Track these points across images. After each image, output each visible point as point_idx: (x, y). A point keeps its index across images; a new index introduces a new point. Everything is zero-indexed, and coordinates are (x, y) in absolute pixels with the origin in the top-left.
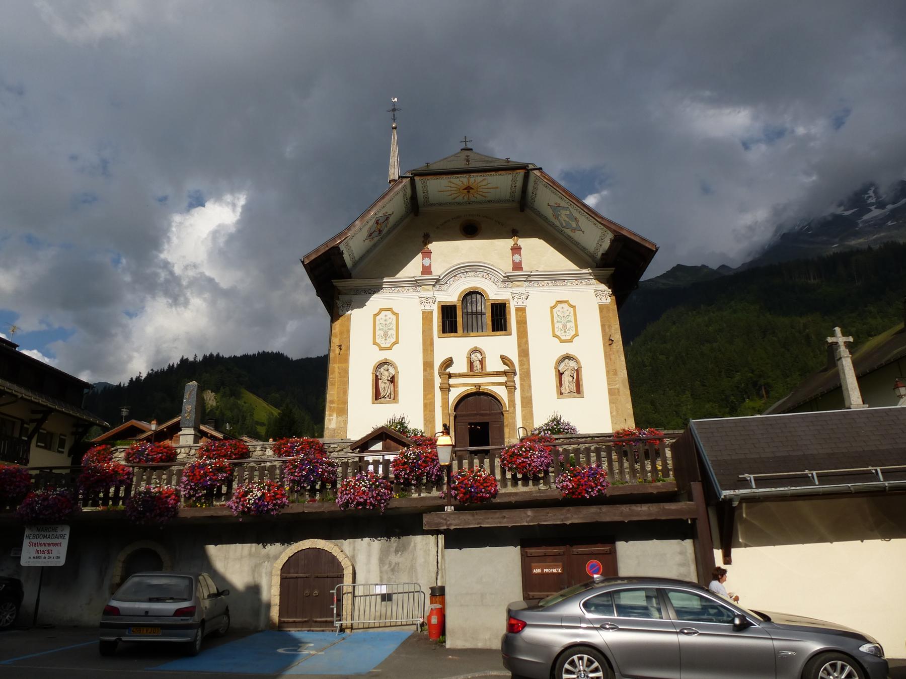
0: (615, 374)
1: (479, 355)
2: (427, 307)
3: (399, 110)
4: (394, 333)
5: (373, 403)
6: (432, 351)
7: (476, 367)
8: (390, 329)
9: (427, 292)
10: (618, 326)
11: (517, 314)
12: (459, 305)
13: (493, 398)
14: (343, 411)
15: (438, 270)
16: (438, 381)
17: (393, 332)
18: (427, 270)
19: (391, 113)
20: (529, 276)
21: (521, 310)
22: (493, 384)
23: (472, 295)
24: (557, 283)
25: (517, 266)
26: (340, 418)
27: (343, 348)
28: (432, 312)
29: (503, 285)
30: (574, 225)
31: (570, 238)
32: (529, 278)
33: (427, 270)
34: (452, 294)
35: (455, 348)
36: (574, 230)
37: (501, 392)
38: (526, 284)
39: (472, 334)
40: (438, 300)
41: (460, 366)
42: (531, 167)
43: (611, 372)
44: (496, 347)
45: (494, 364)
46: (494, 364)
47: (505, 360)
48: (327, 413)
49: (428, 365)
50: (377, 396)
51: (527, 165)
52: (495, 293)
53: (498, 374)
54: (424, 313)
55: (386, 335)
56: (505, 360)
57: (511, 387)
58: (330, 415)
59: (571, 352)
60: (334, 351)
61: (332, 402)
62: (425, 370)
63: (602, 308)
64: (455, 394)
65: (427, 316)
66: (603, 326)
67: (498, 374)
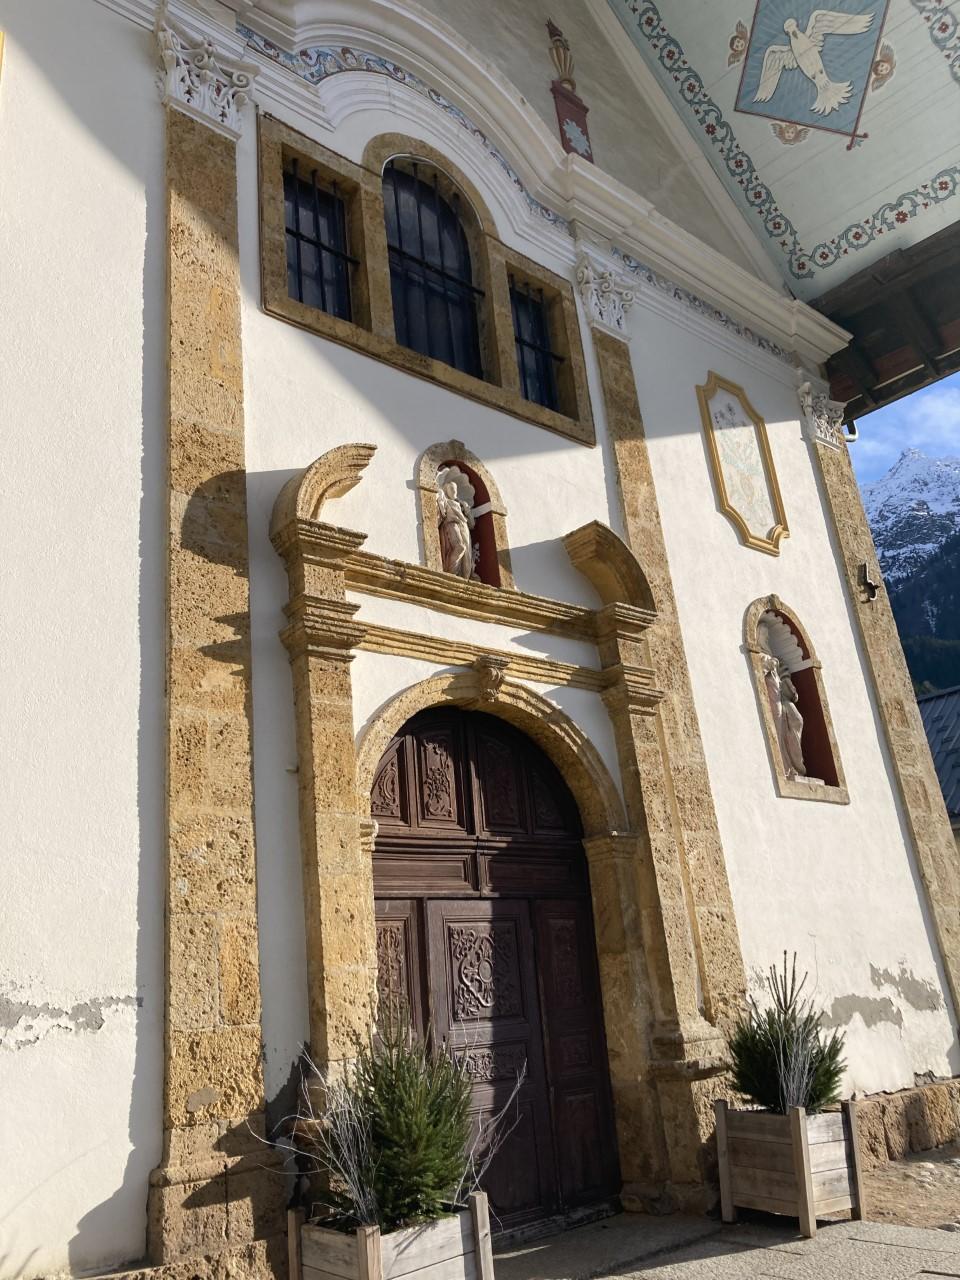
2: (204, 105)
11: (601, 362)
21: (612, 349)
28: (230, 149)
30: (831, 96)
39: (440, 368)
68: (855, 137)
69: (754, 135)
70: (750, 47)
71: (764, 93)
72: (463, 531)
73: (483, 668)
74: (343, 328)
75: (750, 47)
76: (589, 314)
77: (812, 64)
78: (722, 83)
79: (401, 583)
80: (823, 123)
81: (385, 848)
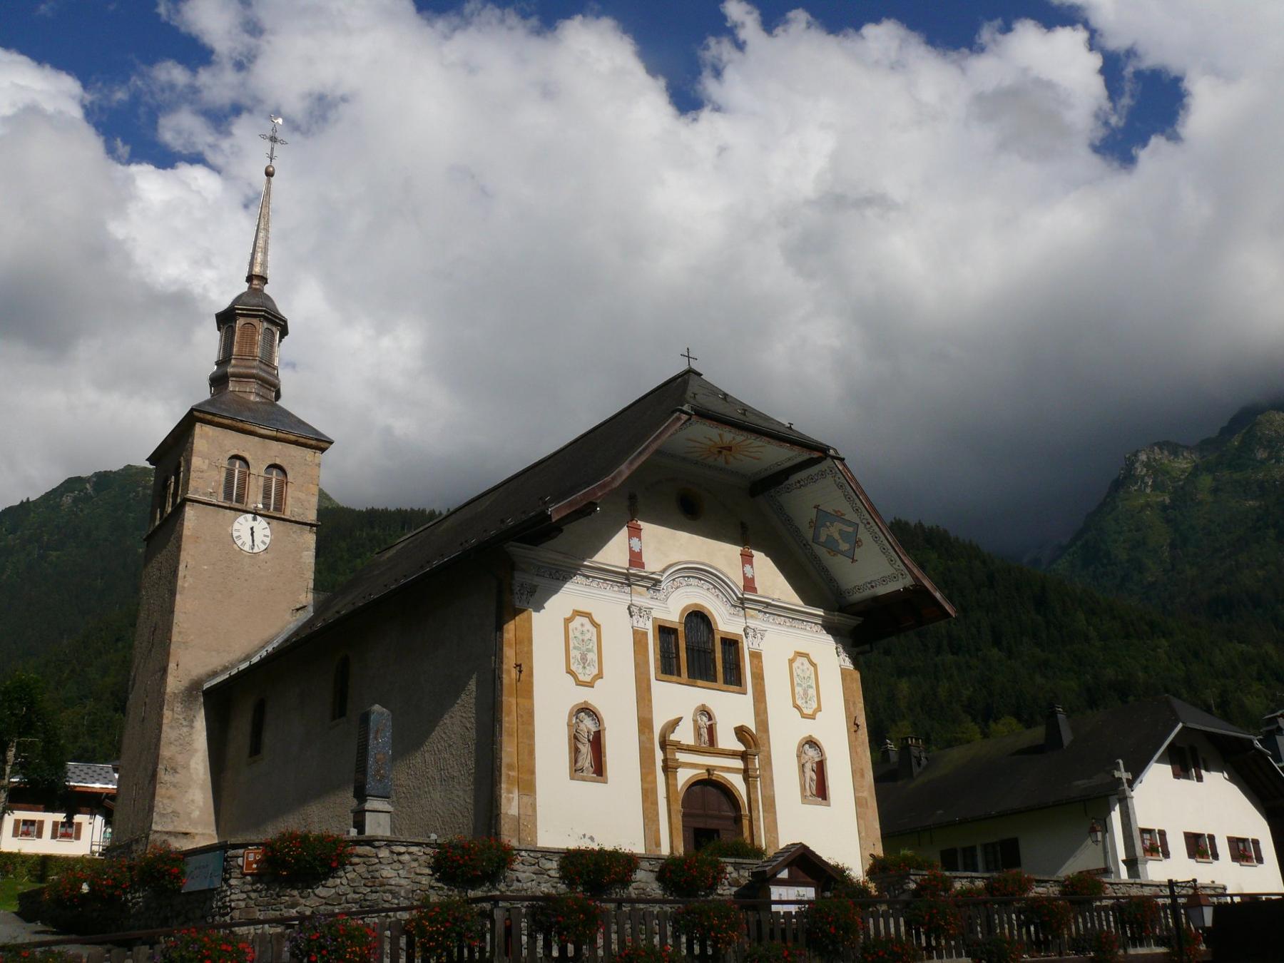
0: (862, 776)
1: (705, 719)
2: (641, 625)
3: (263, 136)
4: (596, 658)
5: (572, 778)
6: (650, 701)
7: (708, 740)
8: (589, 650)
9: (642, 598)
10: (861, 705)
12: (681, 629)
13: (726, 791)
14: (528, 787)
15: (652, 564)
16: (659, 755)
17: (592, 656)
18: (636, 559)
19: (268, 144)
20: (768, 605)
21: (756, 656)
22: (729, 770)
23: (698, 618)
24: (795, 623)
25: (749, 585)
26: (525, 799)
27: (524, 668)
28: (646, 634)
29: (732, 610)
30: (844, 546)
31: (816, 558)
32: (769, 608)
33: (636, 559)
34: (671, 609)
35: (677, 701)
36: (835, 551)
37: (737, 782)
38: (761, 615)
39: (700, 682)
40: (655, 614)
41: (684, 735)
42: (832, 452)
43: (857, 773)
44: (732, 710)
45: (727, 741)
46: (727, 741)
47: (741, 732)
48: (504, 786)
49: (645, 724)
50: (576, 771)
51: (828, 448)
52: (726, 622)
53: (733, 754)
54: (635, 632)
55: (584, 658)
56: (741, 732)
57: (746, 774)
58: (510, 792)
59: (818, 736)
60: (509, 672)
61: (510, 767)
62: (641, 732)
63: (844, 673)
64: (684, 777)
65: (639, 637)
66: (846, 701)
67: (733, 754)
68: (854, 561)
69: (822, 552)
70: (815, 525)
71: (823, 539)
72: (704, 732)
73: (709, 770)
74: (675, 678)
75: (815, 525)
76: (747, 646)
77: (837, 536)
78: (809, 534)
79: (689, 749)
80: (842, 553)
81: (685, 815)
